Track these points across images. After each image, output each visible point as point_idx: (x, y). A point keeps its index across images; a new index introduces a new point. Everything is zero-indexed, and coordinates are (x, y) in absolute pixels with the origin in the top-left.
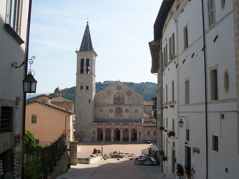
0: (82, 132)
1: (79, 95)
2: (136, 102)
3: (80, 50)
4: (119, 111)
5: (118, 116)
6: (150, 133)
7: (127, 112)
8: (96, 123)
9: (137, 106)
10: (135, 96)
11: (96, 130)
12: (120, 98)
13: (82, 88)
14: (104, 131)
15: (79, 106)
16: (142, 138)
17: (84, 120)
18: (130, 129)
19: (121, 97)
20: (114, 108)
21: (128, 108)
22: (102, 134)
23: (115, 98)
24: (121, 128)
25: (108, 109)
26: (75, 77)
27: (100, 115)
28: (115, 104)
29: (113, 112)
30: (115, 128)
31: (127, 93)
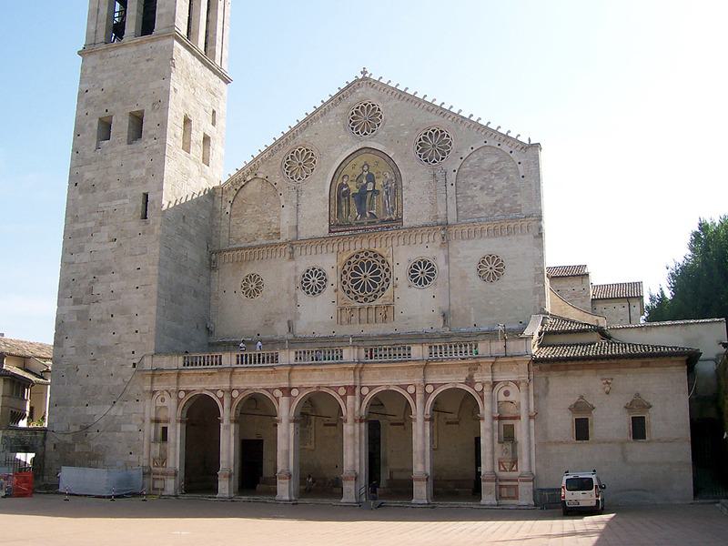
0: (85, 428)
1: (88, 175)
2: (483, 199)
5: (363, 315)
6: (596, 430)
7: (424, 282)
9: (496, 233)
11: (172, 410)
12: (370, 185)
15: (81, 249)
16: (523, 466)
18: (419, 397)
19: (379, 182)
20: (329, 262)
21: (427, 249)
23: (340, 195)
24: (351, 390)
25: (296, 269)
26: (74, 66)
27: (242, 315)
28: (339, 226)
29: (328, 293)
31: (421, 147)
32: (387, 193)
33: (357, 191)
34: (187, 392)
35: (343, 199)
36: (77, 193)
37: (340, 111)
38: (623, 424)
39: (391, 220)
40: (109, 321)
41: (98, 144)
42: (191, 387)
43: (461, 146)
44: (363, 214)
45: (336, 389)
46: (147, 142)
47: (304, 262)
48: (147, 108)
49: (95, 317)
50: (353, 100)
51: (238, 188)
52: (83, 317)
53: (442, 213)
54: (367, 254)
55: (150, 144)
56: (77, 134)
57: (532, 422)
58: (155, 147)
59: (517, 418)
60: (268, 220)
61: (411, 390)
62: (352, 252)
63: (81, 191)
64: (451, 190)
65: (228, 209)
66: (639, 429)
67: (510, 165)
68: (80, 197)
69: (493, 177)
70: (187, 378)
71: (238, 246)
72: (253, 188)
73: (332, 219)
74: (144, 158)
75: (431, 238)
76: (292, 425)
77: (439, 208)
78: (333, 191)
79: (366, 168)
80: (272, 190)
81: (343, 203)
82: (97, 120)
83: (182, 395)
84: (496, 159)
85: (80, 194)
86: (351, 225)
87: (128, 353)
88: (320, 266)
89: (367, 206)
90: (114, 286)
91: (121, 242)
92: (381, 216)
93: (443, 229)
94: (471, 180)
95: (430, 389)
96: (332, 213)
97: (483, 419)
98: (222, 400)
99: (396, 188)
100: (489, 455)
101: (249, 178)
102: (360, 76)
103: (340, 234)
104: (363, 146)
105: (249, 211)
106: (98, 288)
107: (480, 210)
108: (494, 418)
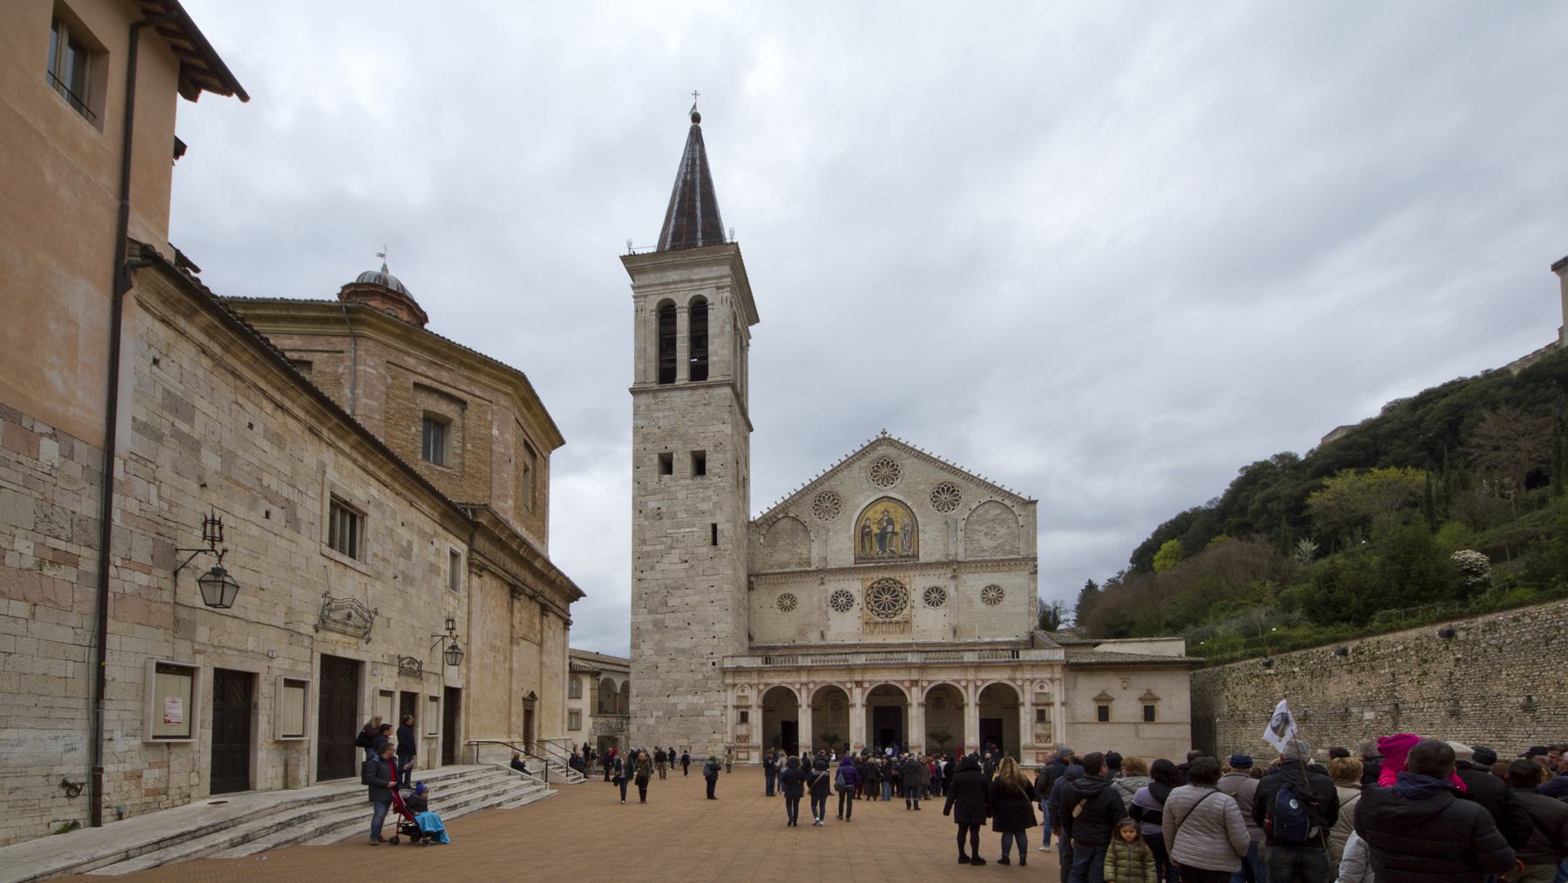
1: (652, 504)
2: (987, 543)
3: (661, 251)
4: (887, 600)
8: (757, 662)
10: (980, 511)
12: (890, 529)
13: (666, 465)
14: (804, 700)
15: (652, 568)
17: (682, 646)
18: (971, 689)
22: (791, 729)
23: (864, 534)
24: (914, 683)
25: (827, 590)
28: (863, 563)
30: (870, 682)
32: (905, 535)
33: (878, 531)
34: (766, 685)
35: (866, 538)
36: (642, 519)
37: (863, 465)
38: (1138, 710)
39: (908, 556)
40: (685, 628)
41: (659, 478)
42: (770, 681)
43: (972, 498)
44: (884, 551)
45: (902, 682)
46: (711, 480)
47: (833, 586)
48: (710, 450)
49: (672, 625)
50: (874, 455)
51: (770, 523)
52: (660, 626)
53: (952, 552)
54: (887, 582)
55: (714, 481)
56: (636, 467)
57: (1063, 708)
58: (721, 484)
59: (1050, 704)
60: (799, 551)
61: (964, 684)
62: (875, 580)
63: (646, 518)
64: (961, 534)
65: (762, 540)
66: (1149, 715)
67: (1011, 516)
68: (647, 523)
69: (996, 525)
70: (766, 675)
71: (772, 571)
72: (785, 524)
74: (709, 493)
75: (943, 571)
76: (864, 709)
77: (951, 548)
78: (857, 531)
79: (886, 513)
80: (801, 527)
81: (866, 541)
82: (657, 455)
83: (762, 687)
84: (999, 511)
85: (645, 520)
86: (873, 558)
87: (708, 654)
88: (848, 590)
90: (687, 600)
91: (693, 563)
92: (899, 551)
93: (953, 566)
94: (977, 527)
95: (979, 683)
96: (857, 549)
97: (1023, 704)
98: (799, 690)
99: (913, 528)
100: (1029, 731)
101: (780, 516)
102: (881, 436)
103: (865, 565)
104: (882, 495)
105: (781, 543)
106: (672, 601)
107: (984, 551)
108: (1033, 704)
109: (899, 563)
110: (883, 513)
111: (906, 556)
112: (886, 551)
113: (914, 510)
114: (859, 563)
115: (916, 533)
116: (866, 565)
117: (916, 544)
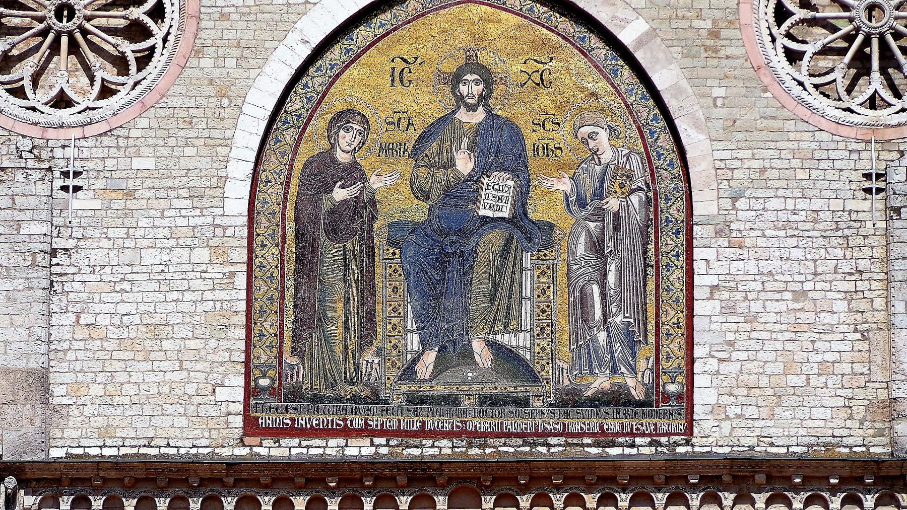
32: (597, 246)
33: (418, 211)
35: (330, 250)
73: (262, 356)
79: (472, 88)
81: (331, 274)
86: (375, 399)
89: (478, 304)
96: (268, 325)
109: (556, 448)
110: (456, 79)
111: (600, 401)
112: (468, 354)
113: (660, 80)
114: (278, 433)
115: (671, 243)
116: (332, 448)
117: (673, 315)
